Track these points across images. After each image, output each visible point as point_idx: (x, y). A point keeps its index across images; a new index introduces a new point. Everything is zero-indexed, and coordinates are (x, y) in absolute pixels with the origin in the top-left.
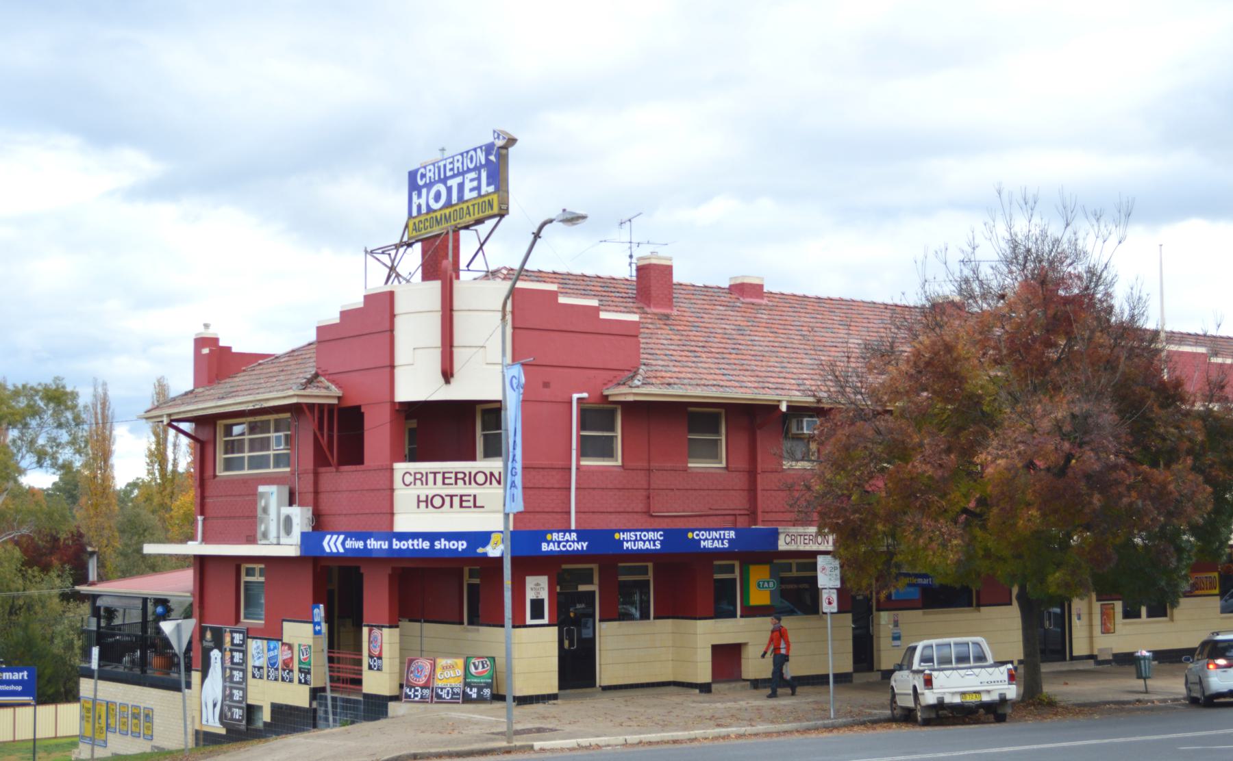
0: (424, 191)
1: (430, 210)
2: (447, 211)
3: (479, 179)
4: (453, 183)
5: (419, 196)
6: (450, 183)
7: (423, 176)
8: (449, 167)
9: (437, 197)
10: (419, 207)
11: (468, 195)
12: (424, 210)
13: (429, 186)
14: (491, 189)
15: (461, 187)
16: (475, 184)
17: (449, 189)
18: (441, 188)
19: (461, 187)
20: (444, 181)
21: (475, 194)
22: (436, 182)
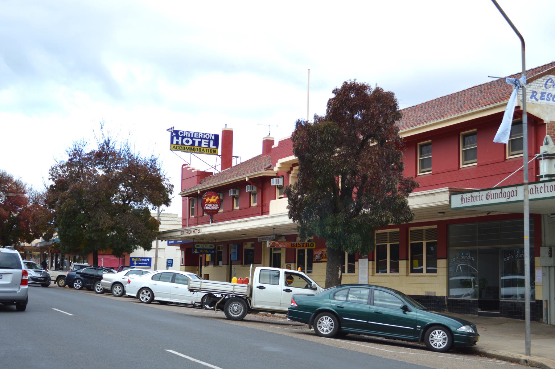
0: (180, 138)
1: (182, 144)
2: (192, 147)
3: (209, 142)
4: (197, 141)
5: (178, 138)
6: (194, 139)
7: (181, 133)
8: (195, 135)
9: (187, 142)
10: (177, 143)
11: (203, 145)
12: (180, 143)
13: (183, 138)
14: (215, 147)
15: (200, 143)
16: (207, 143)
17: (194, 142)
18: (190, 140)
19: (200, 143)
20: (192, 138)
21: (207, 146)
22: (188, 137)
